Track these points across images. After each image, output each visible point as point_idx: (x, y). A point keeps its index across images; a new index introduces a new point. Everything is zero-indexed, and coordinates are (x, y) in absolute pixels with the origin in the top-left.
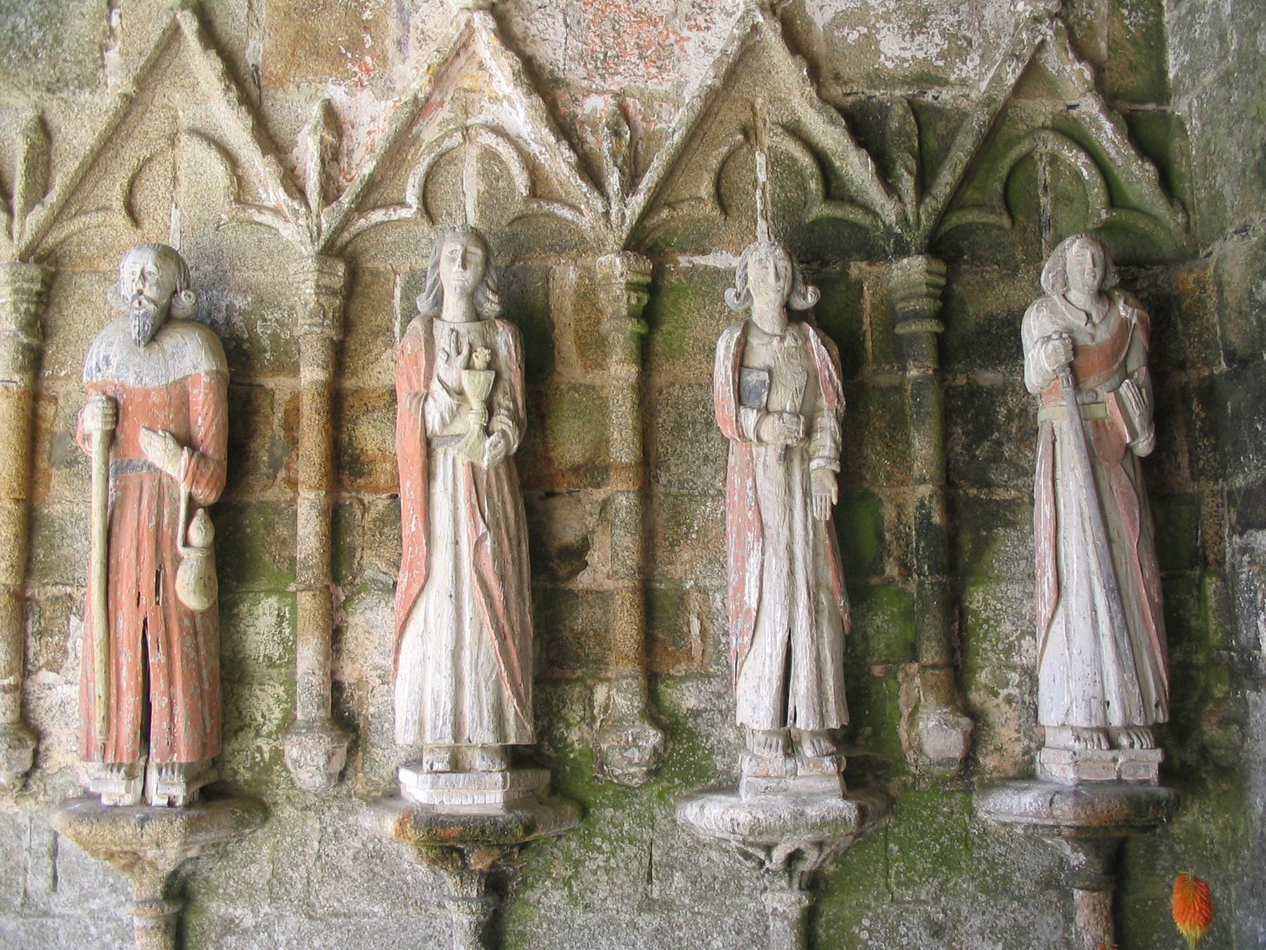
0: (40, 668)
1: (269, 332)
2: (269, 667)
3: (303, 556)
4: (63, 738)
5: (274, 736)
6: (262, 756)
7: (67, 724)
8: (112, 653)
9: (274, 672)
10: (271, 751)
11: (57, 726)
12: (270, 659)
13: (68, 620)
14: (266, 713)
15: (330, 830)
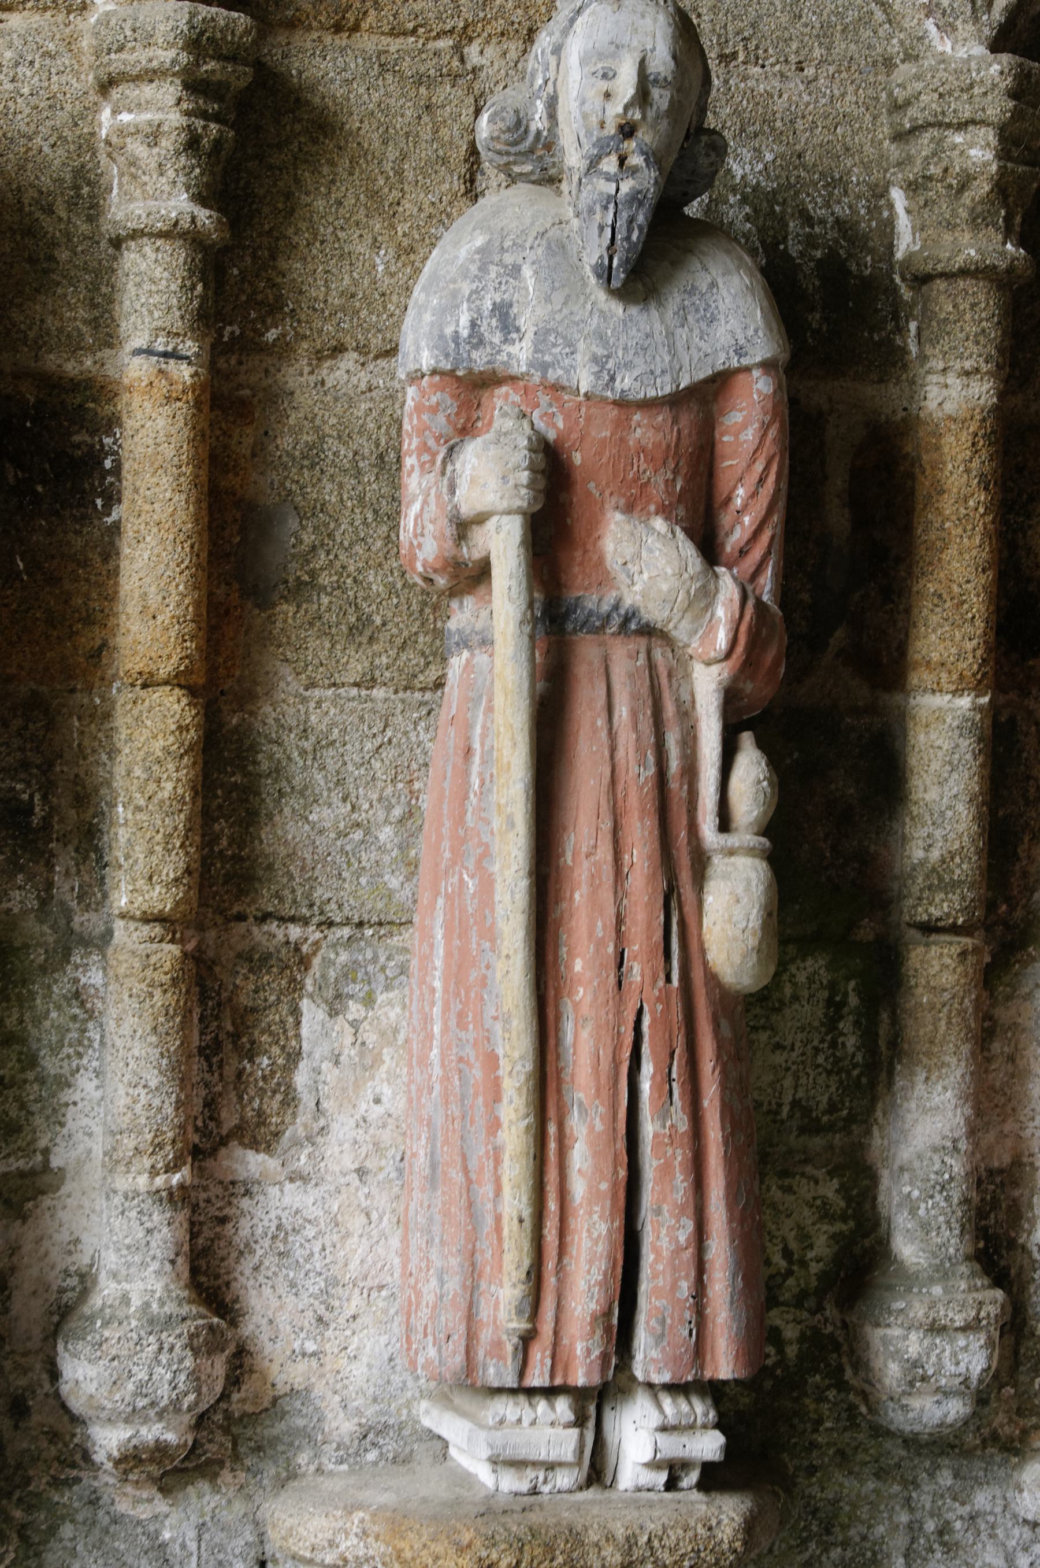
0: (224, 1142)
1: (818, 254)
2: (802, 1130)
3: (935, 854)
4: (283, 1319)
5: (811, 1303)
6: (780, 1351)
7: (293, 1285)
8: (552, 1112)
9: (817, 1143)
10: (802, 1338)
11: (267, 1291)
12: (806, 1111)
13: (296, 1012)
14: (793, 1245)
15: (930, 1526)
